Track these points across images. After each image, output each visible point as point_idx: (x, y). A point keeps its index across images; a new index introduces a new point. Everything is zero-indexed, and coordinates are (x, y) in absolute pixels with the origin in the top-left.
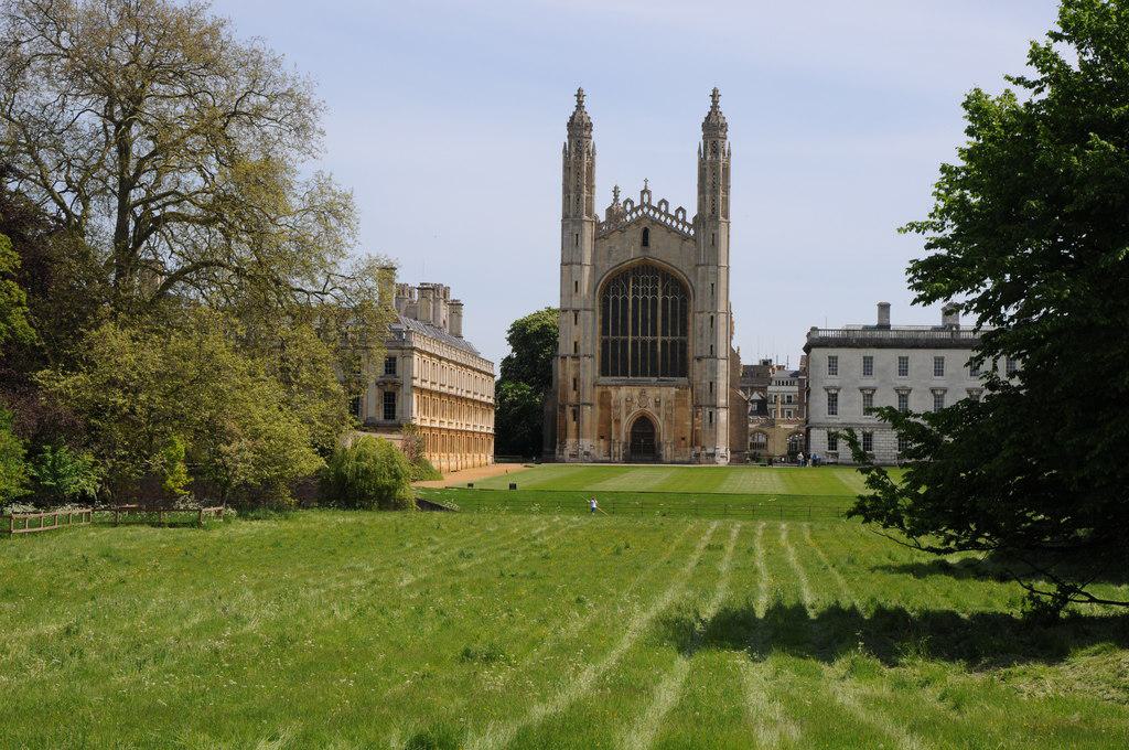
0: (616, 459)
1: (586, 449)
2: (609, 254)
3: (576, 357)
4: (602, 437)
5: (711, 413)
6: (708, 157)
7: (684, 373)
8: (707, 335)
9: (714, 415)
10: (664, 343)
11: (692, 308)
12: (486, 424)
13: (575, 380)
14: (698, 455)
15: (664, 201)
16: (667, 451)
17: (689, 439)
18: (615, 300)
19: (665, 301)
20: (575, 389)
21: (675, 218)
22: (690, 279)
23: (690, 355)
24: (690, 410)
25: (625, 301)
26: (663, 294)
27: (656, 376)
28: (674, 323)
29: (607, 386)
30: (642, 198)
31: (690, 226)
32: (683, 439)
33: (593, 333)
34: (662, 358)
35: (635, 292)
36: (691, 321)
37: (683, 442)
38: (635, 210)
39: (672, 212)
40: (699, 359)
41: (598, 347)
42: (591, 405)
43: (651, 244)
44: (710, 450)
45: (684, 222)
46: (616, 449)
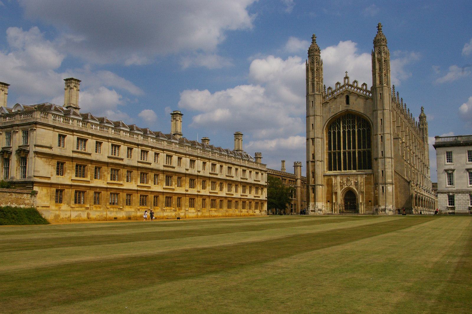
0: (336, 212)
1: (320, 208)
2: (330, 109)
3: (313, 162)
4: (329, 202)
5: (383, 187)
6: (376, 56)
7: (370, 167)
8: (380, 146)
9: (384, 188)
10: (359, 152)
11: (372, 134)
12: (263, 195)
13: (313, 173)
14: (377, 210)
15: (355, 82)
16: (362, 209)
17: (373, 202)
18: (334, 133)
19: (359, 131)
20: (313, 178)
21: (361, 89)
22: (370, 118)
23: (373, 158)
24: (373, 186)
25: (339, 133)
26: (358, 128)
27: (355, 169)
28: (364, 142)
29: (330, 175)
30: (344, 81)
31: (370, 92)
32: (370, 201)
33: (323, 149)
34: (359, 160)
35: (344, 128)
36: (372, 141)
37: (370, 203)
38: (341, 88)
39: (360, 86)
40: (376, 159)
41: (326, 157)
42: (322, 185)
43: (350, 103)
44: (383, 207)
45: (367, 91)
46: (336, 207)
